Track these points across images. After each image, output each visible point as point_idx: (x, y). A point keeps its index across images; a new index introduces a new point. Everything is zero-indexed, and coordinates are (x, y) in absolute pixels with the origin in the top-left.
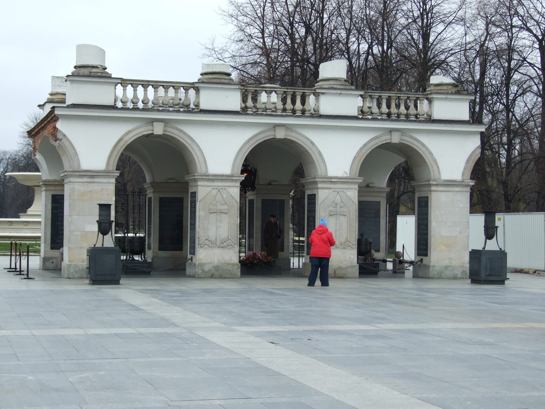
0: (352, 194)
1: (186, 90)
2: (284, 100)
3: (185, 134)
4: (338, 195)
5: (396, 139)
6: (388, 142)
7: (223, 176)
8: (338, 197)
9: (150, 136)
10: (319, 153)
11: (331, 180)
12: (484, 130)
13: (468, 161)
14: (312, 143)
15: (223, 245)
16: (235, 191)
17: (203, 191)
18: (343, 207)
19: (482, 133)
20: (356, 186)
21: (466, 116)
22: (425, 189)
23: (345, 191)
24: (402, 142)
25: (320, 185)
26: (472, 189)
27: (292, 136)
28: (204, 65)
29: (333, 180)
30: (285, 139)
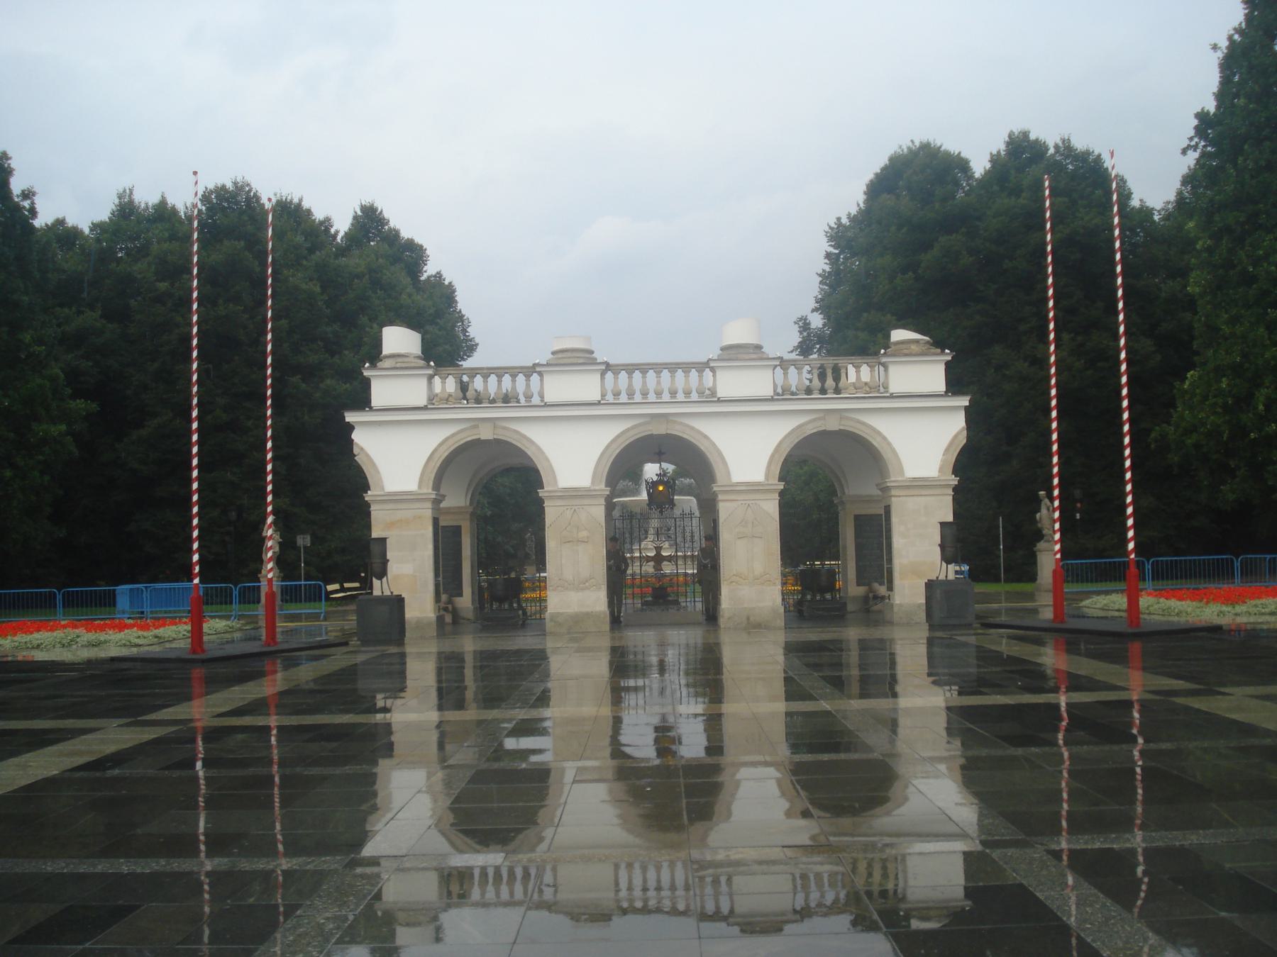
0: (771, 507)
1: (528, 377)
2: (822, 377)
3: (524, 437)
9: (651, 436)
13: (947, 450)
14: (706, 437)
15: (581, 585)
17: (552, 513)
19: (966, 408)
20: (776, 496)
21: (941, 386)
25: (720, 497)
26: (955, 489)
27: (676, 430)
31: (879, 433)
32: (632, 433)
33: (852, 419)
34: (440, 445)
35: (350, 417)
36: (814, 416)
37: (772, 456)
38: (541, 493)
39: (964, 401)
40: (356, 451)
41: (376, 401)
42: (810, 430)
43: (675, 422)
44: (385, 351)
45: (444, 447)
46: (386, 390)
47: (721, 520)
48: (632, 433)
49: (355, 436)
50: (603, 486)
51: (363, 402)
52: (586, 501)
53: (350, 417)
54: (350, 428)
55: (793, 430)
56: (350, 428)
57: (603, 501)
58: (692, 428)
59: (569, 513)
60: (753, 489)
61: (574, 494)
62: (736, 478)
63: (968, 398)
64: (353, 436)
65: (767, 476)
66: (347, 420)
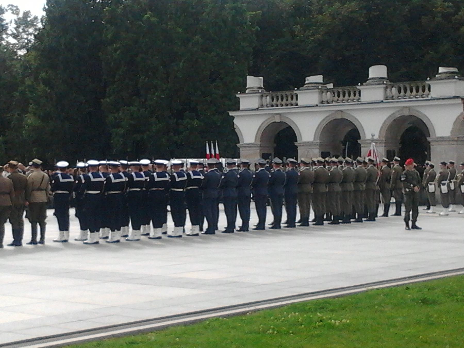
14: (357, 120)
25: (362, 145)
34: (263, 124)
35: (231, 114)
38: (296, 144)
40: (235, 127)
41: (241, 107)
46: (247, 102)
49: (235, 121)
51: (237, 108)
53: (231, 114)
54: (233, 118)
56: (233, 118)
57: (318, 147)
61: (308, 144)
64: (234, 121)
66: (230, 115)
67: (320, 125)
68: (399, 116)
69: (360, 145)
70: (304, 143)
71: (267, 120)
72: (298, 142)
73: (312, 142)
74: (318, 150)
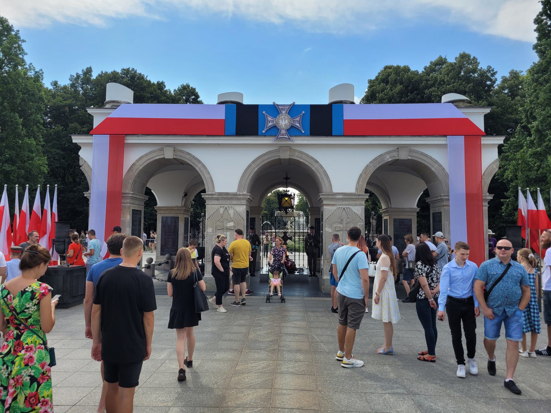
3: (194, 157)
4: (344, 211)
5: (404, 156)
6: (395, 158)
7: (227, 194)
8: (344, 213)
10: (325, 172)
11: (333, 196)
12: (502, 142)
14: (317, 162)
16: (242, 209)
17: (211, 208)
18: (349, 223)
19: (500, 147)
22: (438, 204)
23: (350, 207)
24: (410, 158)
25: (325, 202)
27: (296, 157)
28: (219, 96)
29: (338, 197)
30: (290, 159)
31: (436, 162)
32: (266, 157)
33: (417, 152)
35: (76, 139)
36: (391, 149)
37: (361, 175)
39: (500, 140)
40: (81, 163)
42: (388, 158)
43: (295, 150)
44: (107, 99)
45: (141, 162)
47: (325, 218)
48: (266, 157)
49: (80, 153)
50: (245, 193)
52: (234, 202)
53: (76, 139)
54: (77, 148)
55: (376, 159)
56: (77, 148)
57: (244, 202)
58: (307, 155)
59: (222, 210)
60: (347, 197)
62: (335, 190)
63: (503, 138)
65: (357, 189)
67: (250, 166)
68: (390, 160)
69: (322, 201)
70: (220, 194)
71: (146, 155)
72: (207, 193)
73: (235, 194)
74: (245, 207)
